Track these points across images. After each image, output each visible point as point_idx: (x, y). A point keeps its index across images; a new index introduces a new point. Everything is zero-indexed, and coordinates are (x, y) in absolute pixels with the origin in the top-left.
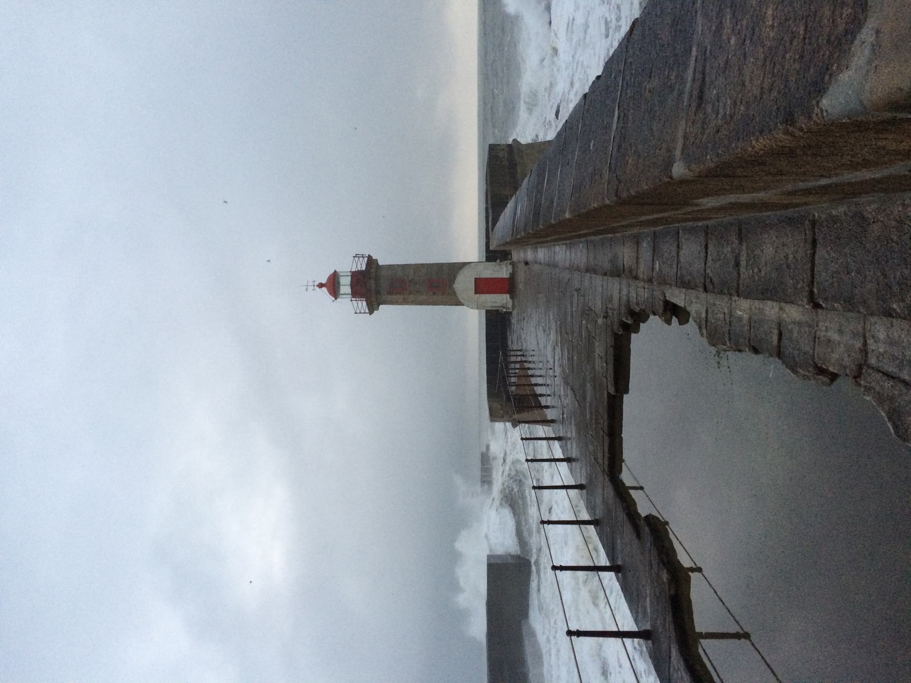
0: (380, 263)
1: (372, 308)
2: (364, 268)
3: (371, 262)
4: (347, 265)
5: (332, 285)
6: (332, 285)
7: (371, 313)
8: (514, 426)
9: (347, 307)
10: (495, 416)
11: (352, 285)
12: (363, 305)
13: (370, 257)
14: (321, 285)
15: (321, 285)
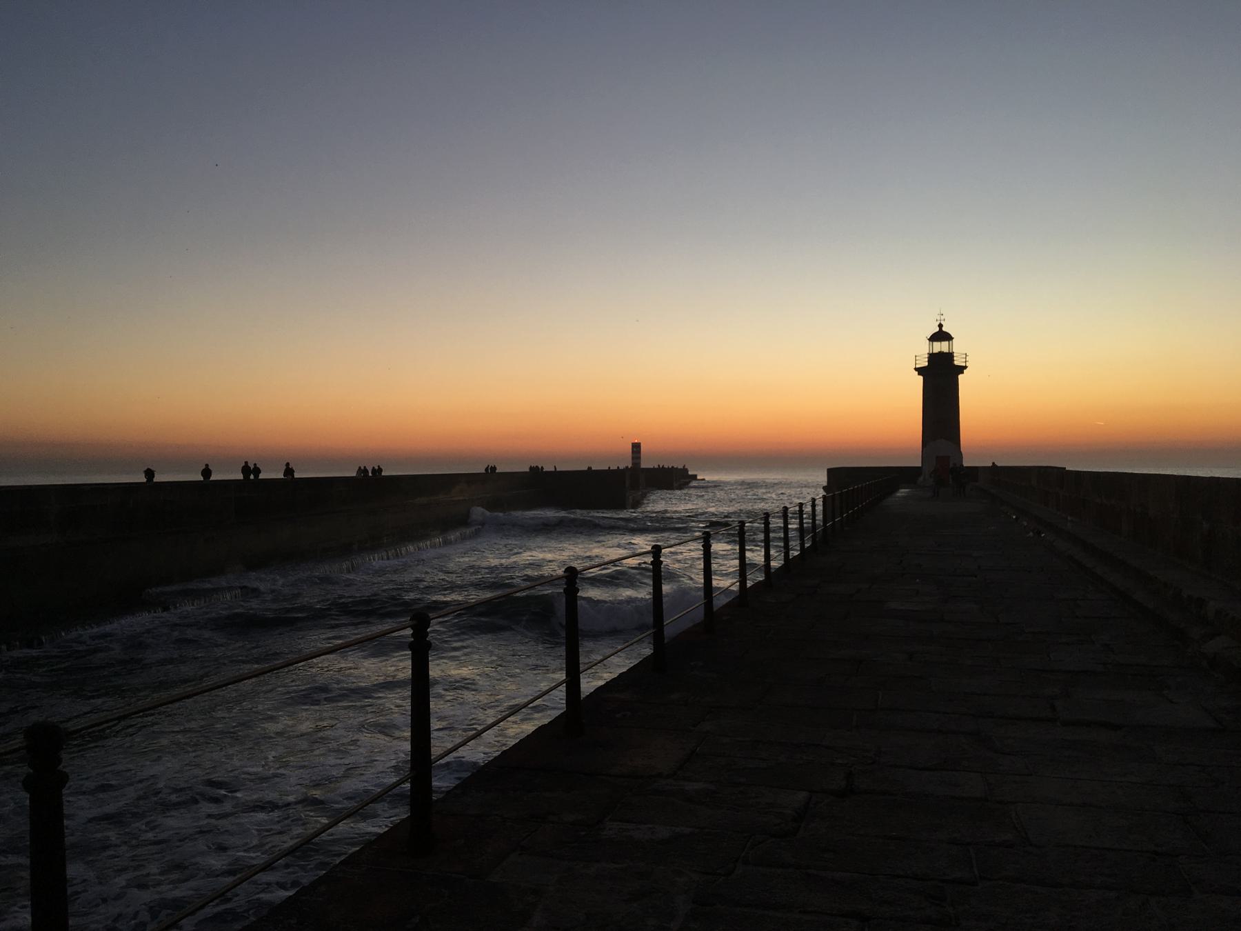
0: (960, 376)
1: (920, 371)
2: (956, 363)
3: (961, 369)
4: (959, 349)
5: (941, 336)
6: (941, 336)
7: (916, 369)
8: (824, 488)
9: (921, 351)
10: (831, 472)
11: (941, 353)
12: (924, 363)
13: (965, 367)
14: (940, 326)
15: (940, 326)
